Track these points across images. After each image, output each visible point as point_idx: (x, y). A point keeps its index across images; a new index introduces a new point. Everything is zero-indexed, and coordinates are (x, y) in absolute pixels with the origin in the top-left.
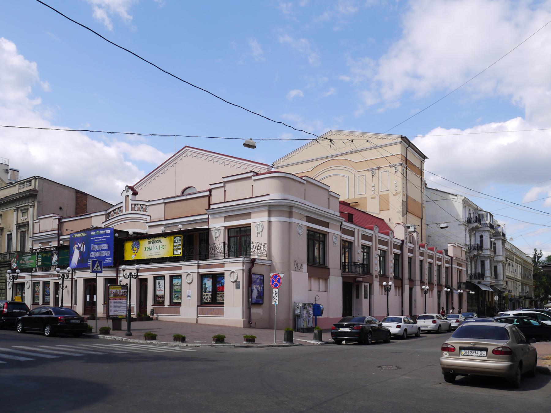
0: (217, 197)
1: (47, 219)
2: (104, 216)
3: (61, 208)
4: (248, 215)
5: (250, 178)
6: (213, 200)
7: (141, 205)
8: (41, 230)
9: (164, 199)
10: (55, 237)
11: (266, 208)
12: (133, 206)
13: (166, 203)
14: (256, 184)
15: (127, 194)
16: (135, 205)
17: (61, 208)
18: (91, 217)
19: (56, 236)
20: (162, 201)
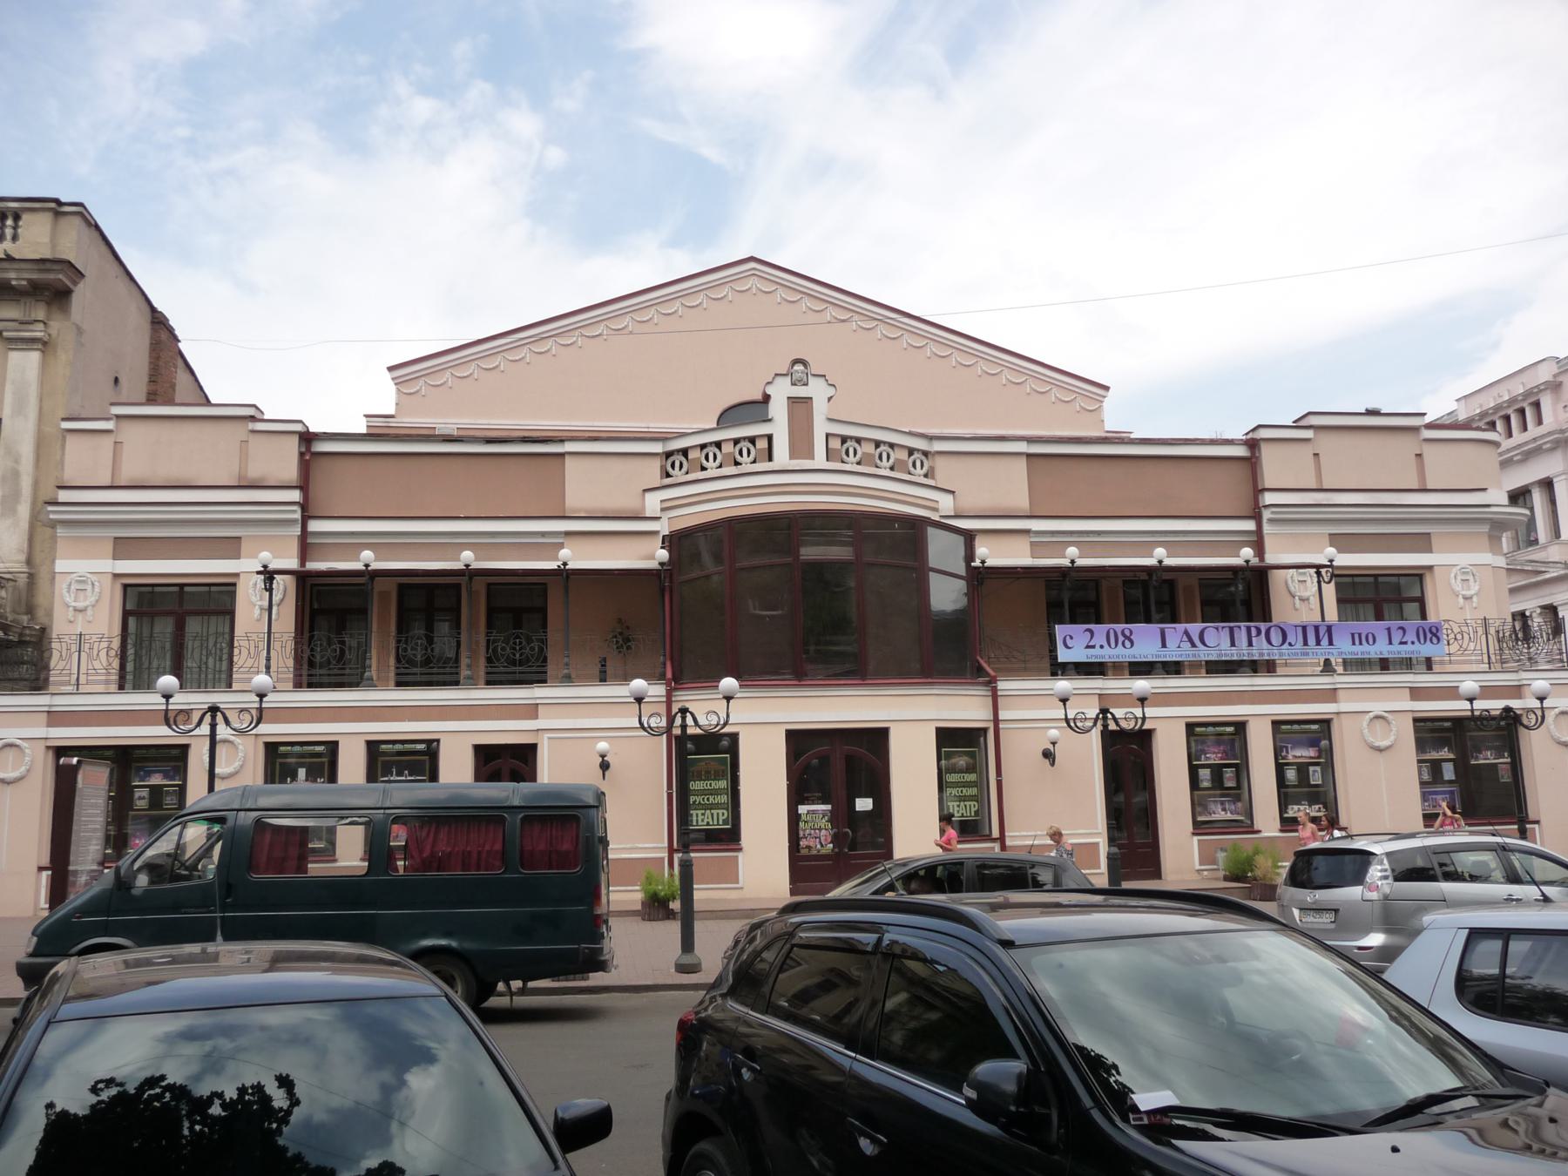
0: (1274, 468)
1: (177, 425)
2: (655, 466)
3: (116, 380)
4: (1422, 543)
5: (1430, 426)
6: (1269, 477)
7: (878, 444)
8: (127, 474)
9: (1030, 440)
10: (294, 521)
11: (1486, 528)
12: (835, 444)
13: (1029, 456)
14: (1429, 452)
15: (800, 392)
16: (844, 440)
17: (116, 380)
18: (562, 455)
19: (298, 516)
20: (1022, 447)
